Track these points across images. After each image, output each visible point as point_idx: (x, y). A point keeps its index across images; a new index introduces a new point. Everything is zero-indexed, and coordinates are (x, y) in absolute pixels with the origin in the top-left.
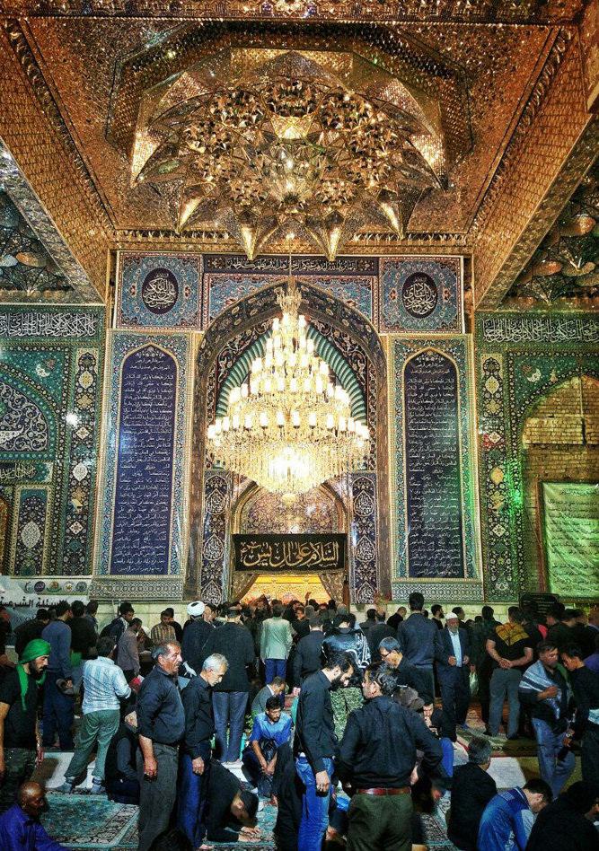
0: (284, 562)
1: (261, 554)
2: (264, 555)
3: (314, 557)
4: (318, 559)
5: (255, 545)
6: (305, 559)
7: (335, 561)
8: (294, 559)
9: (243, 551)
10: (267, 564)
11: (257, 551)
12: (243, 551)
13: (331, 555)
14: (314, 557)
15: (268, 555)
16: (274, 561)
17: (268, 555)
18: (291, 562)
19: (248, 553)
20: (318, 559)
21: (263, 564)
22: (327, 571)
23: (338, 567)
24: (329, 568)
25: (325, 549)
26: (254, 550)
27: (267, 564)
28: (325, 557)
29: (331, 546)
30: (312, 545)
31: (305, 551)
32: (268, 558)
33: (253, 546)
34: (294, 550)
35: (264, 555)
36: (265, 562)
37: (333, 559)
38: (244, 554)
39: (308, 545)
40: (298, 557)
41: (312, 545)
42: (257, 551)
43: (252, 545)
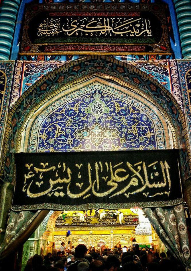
0: (90, 191)
1: (54, 179)
2: (59, 180)
3: (134, 182)
4: (140, 185)
5: (47, 167)
6: (121, 185)
7: (166, 188)
8: (104, 187)
9: (27, 177)
10: (62, 194)
11: (49, 176)
12: (27, 177)
13: (159, 179)
14: (134, 182)
15: (65, 180)
16: (75, 190)
17: (65, 180)
18: (99, 192)
19: (36, 178)
20: (140, 185)
21: (57, 194)
22: (156, 204)
23: (172, 197)
24: (158, 199)
25: (150, 171)
26: (44, 174)
27: (62, 194)
28: (151, 182)
29: (158, 166)
30: (129, 165)
31: (121, 175)
32: (64, 185)
33: (44, 168)
34: (105, 173)
35: (59, 180)
36: (59, 191)
37: (163, 185)
38: (29, 180)
39: (124, 166)
40: (110, 183)
41: (129, 165)
42: (49, 176)
43: (42, 167)
